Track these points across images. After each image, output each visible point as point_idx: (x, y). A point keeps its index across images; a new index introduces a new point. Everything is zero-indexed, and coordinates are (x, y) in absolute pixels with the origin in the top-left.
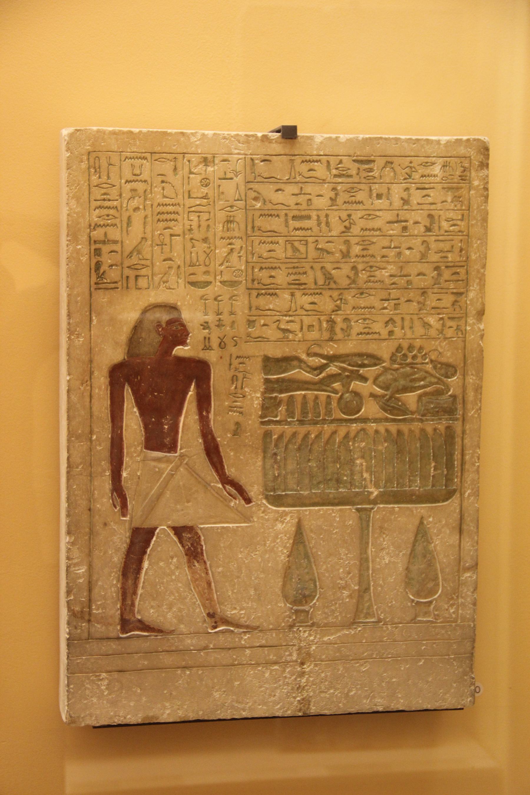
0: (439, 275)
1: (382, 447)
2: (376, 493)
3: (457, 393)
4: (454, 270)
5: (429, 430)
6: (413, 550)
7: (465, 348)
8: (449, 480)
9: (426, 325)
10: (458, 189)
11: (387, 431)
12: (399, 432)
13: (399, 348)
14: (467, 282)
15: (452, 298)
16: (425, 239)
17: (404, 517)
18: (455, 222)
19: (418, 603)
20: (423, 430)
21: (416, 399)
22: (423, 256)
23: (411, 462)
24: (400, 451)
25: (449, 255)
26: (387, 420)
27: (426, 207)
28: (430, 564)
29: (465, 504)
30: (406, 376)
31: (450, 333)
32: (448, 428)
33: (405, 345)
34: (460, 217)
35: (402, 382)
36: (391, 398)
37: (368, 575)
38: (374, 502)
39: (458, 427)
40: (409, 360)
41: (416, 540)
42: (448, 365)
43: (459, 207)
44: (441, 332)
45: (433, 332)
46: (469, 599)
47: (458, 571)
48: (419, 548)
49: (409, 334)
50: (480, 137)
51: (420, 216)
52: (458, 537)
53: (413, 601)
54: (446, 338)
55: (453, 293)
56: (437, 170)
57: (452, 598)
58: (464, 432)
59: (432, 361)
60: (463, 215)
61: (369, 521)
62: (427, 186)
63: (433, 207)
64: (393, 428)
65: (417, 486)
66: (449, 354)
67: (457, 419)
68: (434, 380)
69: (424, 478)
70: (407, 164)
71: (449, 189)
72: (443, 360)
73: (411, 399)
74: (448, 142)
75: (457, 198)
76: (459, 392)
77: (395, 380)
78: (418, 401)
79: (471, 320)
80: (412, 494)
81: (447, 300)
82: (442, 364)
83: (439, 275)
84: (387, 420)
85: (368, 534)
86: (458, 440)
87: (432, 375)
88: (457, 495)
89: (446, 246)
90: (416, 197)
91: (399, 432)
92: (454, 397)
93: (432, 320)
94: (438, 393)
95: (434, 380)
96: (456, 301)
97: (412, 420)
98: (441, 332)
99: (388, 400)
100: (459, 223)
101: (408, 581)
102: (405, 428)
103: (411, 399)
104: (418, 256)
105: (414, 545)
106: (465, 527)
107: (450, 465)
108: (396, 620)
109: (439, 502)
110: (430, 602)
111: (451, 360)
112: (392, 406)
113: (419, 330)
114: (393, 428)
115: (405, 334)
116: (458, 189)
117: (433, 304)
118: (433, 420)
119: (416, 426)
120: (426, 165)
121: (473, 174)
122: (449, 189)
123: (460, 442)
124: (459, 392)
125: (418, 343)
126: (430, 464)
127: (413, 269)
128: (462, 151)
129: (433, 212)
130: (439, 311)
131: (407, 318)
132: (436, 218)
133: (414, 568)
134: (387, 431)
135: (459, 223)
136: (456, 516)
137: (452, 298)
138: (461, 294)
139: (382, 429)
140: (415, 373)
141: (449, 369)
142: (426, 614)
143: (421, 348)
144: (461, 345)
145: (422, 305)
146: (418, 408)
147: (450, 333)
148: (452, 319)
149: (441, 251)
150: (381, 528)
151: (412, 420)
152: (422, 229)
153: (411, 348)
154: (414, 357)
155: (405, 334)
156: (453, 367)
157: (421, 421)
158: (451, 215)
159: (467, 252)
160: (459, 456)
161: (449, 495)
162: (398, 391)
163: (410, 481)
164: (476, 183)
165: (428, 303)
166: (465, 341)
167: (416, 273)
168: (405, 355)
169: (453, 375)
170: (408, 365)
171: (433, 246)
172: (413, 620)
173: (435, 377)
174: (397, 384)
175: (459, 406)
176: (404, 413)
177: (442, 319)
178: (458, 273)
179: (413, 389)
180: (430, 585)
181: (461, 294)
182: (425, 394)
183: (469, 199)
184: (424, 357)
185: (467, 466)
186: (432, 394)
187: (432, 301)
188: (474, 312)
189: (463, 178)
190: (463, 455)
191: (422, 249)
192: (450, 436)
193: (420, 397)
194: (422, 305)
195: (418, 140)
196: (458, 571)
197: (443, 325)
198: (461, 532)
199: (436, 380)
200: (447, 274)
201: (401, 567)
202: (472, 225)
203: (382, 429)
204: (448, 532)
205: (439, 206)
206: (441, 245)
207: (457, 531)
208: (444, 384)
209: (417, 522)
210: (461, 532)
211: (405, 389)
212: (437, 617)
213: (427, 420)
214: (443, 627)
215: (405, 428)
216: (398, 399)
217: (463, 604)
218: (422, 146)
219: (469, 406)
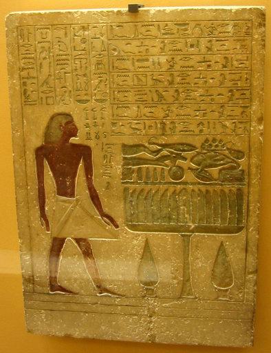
0: (232, 95)
1: (197, 200)
2: (193, 226)
3: (244, 168)
4: (242, 92)
5: (227, 191)
6: (216, 261)
7: (250, 141)
8: (239, 221)
9: (224, 126)
10: (244, 40)
11: (199, 190)
12: (207, 191)
13: (207, 141)
14: (251, 100)
15: (241, 110)
16: (223, 72)
17: (210, 241)
18: (242, 62)
19: (219, 290)
20: (222, 190)
21: (218, 171)
22: (222, 83)
23: (215, 210)
24: (208, 202)
25: (239, 83)
26: (199, 183)
27: (223, 52)
28: (227, 269)
29: (250, 235)
30: (211, 157)
31: (240, 131)
32: (239, 190)
33: (211, 139)
34: (245, 58)
35: (209, 161)
36: (202, 170)
37: (189, 273)
38: (193, 231)
39: (245, 189)
40: (213, 148)
41: (218, 255)
42: (239, 151)
43: (245, 52)
44: (234, 131)
45: (228, 131)
46: (251, 290)
47: (245, 273)
48: (220, 259)
49: (213, 132)
50: (258, 7)
51: (218, 58)
52: (244, 254)
53: (216, 288)
54: (237, 135)
55: (241, 107)
56: (230, 28)
57: (241, 289)
58: (249, 193)
59: (228, 149)
60: (247, 57)
61: (189, 242)
62: (223, 39)
63: (227, 52)
64: (203, 188)
65: (218, 224)
66: (239, 144)
67: (245, 185)
68: (229, 160)
69: (224, 219)
70: (210, 25)
71: (238, 40)
72: (235, 148)
73: (214, 171)
74: (237, 10)
75: (243, 46)
76: (246, 168)
77: (205, 160)
78: (219, 173)
79: (254, 124)
80: (216, 228)
81: (238, 111)
82: (235, 150)
83: (232, 95)
84: (199, 183)
85: (189, 249)
86: (245, 198)
87: (228, 158)
88: (245, 230)
89: (237, 77)
90: (216, 46)
91: (207, 191)
92: (243, 171)
93: (227, 124)
94: (233, 168)
95: (229, 160)
96: (244, 112)
97: (216, 184)
98: (234, 131)
99: (199, 172)
100: (245, 62)
101: (213, 277)
102: (210, 189)
103: (214, 171)
104: (218, 83)
105: (217, 257)
106: (249, 248)
107: (240, 212)
108: (206, 298)
109: (233, 233)
110: (227, 290)
111: (240, 149)
112: (203, 175)
113: (219, 130)
114: (203, 188)
115: (210, 132)
116: (244, 40)
117: (229, 114)
118: (229, 185)
119: (218, 188)
120: (223, 25)
121: (254, 30)
122: (238, 40)
123: (246, 199)
124: (246, 168)
125: (218, 137)
126: (227, 211)
127: (215, 92)
128: (247, 16)
129: (226, 56)
130: (232, 118)
131: (212, 122)
132: (230, 59)
133: (218, 270)
134: (199, 190)
135: (245, 62)
136: (244, 242)
137: (241, 110)
138: (247, 107)
139: (196, 190)
140: (217, 156)
141: (239, 154)
142: (224, 296)
143: (221, 141)
144: (247, 139)
145: (221, 114)
146: (219, 177)
147: (240, 131)
148: (241, 122)
149: (233, 80)
150: (197, 246)
151: (216, 184)
152: (221, 66)
153: (214, 140)
154: (217, 146)
155: (210, 132)
156: (242, 152)
157: (222, 185)
158: (240, 57)
159: (250, 81)
160: (246, 207)
161: (240, 229)
162: (206, 167)
163: (214, 220)
164: (256, 37)
165: (225, 112)
166: (249, 137)
167: (217, 93)
168: (210, 145)
169: (242, 157)
170: (212, 151)
171: (228, 77)
172: (217, 299)
173: (230, 159)
174: (205, 162)
175: (246, 177)
176: (210, 180)
177: (234, 122)
178: (245, 94)
179: (216, 166)
180: (227, 280)
181: (247, 107)
182: (224, 169)
183: (252, 47)
184: (223, 146)
185: (251, 213)
186: (228, 169)
187: (227, 112)
188: (256, 119)
189: (247, 34)
190: (248, 206)
191: (221, 78)
192: (240, 194)
193: (220, 170)
194: (221, 114)
195: (216, 10)
196: (245, 273)
197: (235, 127)
198: (246, 251)
199: (230, 161)
200: (237, 95)
201: (209, 270)
202: (254, 64)
203: (196, 190)
204: (238, 251)
205: (231, 52)
206: (233, 76)
207: (245, 251)
208: (236, 163)
209: (219, 245)
210: (246, 251)
211: (211, 166)
212: (231, 298)
213: (225, 185)
214: (234, 304)
215: (210, 189)
216: (206, 171)
217: (247, 293)
218: (220, 14)
219: (252, 177)
